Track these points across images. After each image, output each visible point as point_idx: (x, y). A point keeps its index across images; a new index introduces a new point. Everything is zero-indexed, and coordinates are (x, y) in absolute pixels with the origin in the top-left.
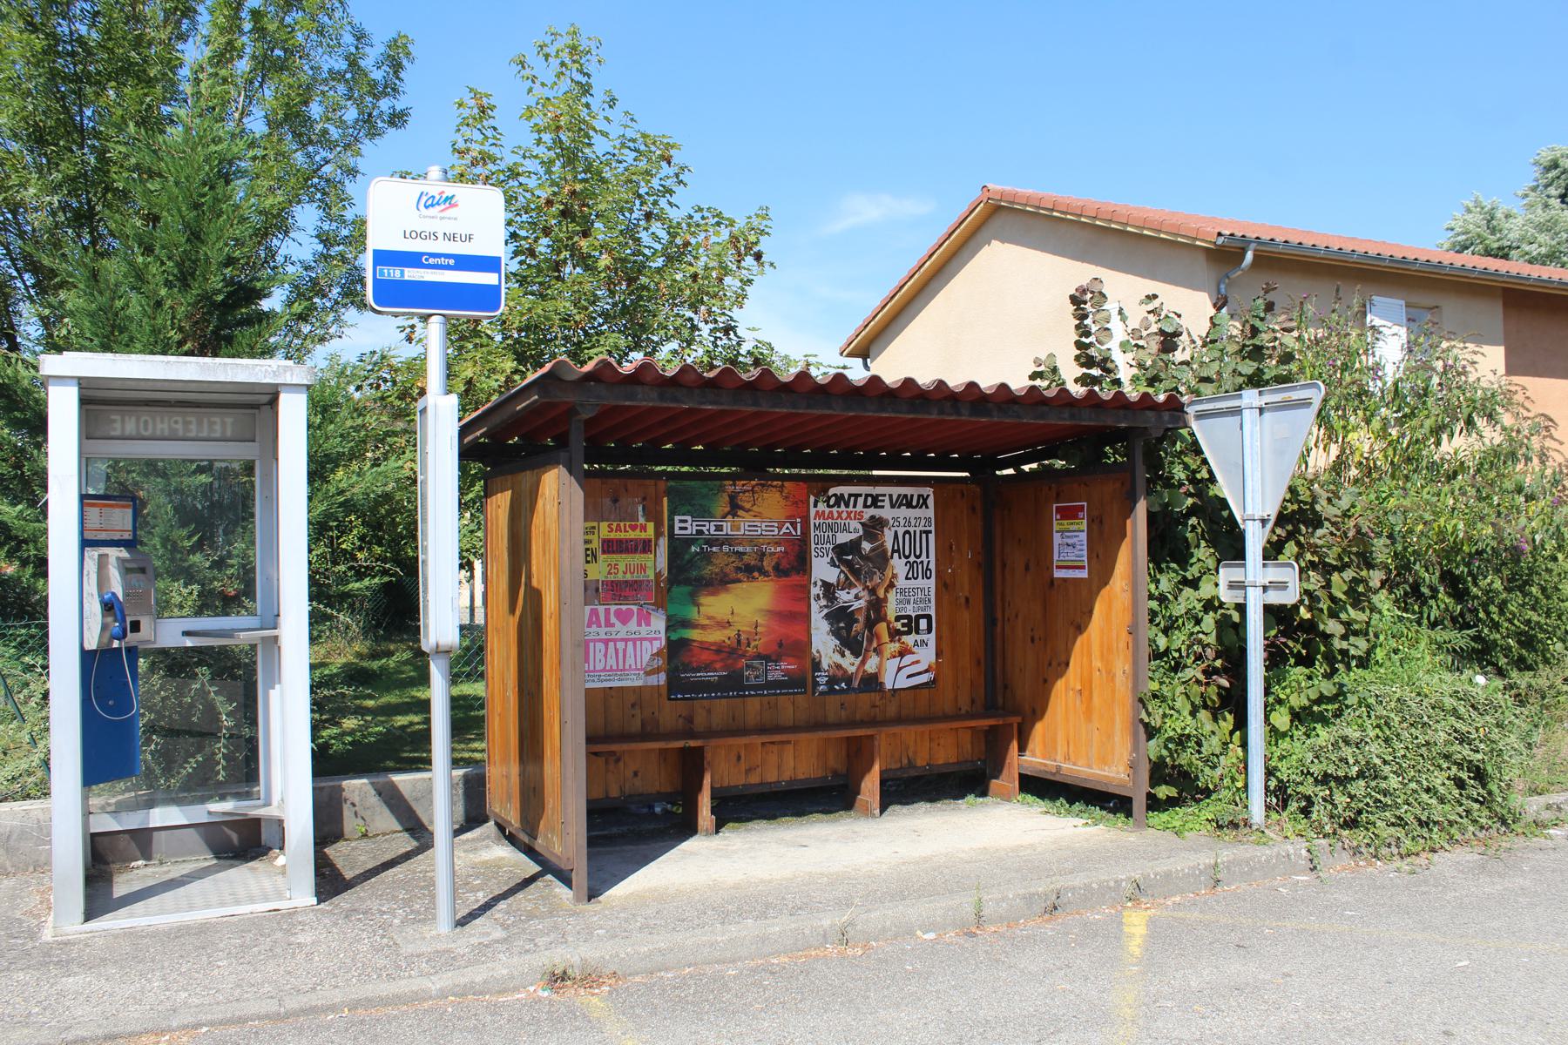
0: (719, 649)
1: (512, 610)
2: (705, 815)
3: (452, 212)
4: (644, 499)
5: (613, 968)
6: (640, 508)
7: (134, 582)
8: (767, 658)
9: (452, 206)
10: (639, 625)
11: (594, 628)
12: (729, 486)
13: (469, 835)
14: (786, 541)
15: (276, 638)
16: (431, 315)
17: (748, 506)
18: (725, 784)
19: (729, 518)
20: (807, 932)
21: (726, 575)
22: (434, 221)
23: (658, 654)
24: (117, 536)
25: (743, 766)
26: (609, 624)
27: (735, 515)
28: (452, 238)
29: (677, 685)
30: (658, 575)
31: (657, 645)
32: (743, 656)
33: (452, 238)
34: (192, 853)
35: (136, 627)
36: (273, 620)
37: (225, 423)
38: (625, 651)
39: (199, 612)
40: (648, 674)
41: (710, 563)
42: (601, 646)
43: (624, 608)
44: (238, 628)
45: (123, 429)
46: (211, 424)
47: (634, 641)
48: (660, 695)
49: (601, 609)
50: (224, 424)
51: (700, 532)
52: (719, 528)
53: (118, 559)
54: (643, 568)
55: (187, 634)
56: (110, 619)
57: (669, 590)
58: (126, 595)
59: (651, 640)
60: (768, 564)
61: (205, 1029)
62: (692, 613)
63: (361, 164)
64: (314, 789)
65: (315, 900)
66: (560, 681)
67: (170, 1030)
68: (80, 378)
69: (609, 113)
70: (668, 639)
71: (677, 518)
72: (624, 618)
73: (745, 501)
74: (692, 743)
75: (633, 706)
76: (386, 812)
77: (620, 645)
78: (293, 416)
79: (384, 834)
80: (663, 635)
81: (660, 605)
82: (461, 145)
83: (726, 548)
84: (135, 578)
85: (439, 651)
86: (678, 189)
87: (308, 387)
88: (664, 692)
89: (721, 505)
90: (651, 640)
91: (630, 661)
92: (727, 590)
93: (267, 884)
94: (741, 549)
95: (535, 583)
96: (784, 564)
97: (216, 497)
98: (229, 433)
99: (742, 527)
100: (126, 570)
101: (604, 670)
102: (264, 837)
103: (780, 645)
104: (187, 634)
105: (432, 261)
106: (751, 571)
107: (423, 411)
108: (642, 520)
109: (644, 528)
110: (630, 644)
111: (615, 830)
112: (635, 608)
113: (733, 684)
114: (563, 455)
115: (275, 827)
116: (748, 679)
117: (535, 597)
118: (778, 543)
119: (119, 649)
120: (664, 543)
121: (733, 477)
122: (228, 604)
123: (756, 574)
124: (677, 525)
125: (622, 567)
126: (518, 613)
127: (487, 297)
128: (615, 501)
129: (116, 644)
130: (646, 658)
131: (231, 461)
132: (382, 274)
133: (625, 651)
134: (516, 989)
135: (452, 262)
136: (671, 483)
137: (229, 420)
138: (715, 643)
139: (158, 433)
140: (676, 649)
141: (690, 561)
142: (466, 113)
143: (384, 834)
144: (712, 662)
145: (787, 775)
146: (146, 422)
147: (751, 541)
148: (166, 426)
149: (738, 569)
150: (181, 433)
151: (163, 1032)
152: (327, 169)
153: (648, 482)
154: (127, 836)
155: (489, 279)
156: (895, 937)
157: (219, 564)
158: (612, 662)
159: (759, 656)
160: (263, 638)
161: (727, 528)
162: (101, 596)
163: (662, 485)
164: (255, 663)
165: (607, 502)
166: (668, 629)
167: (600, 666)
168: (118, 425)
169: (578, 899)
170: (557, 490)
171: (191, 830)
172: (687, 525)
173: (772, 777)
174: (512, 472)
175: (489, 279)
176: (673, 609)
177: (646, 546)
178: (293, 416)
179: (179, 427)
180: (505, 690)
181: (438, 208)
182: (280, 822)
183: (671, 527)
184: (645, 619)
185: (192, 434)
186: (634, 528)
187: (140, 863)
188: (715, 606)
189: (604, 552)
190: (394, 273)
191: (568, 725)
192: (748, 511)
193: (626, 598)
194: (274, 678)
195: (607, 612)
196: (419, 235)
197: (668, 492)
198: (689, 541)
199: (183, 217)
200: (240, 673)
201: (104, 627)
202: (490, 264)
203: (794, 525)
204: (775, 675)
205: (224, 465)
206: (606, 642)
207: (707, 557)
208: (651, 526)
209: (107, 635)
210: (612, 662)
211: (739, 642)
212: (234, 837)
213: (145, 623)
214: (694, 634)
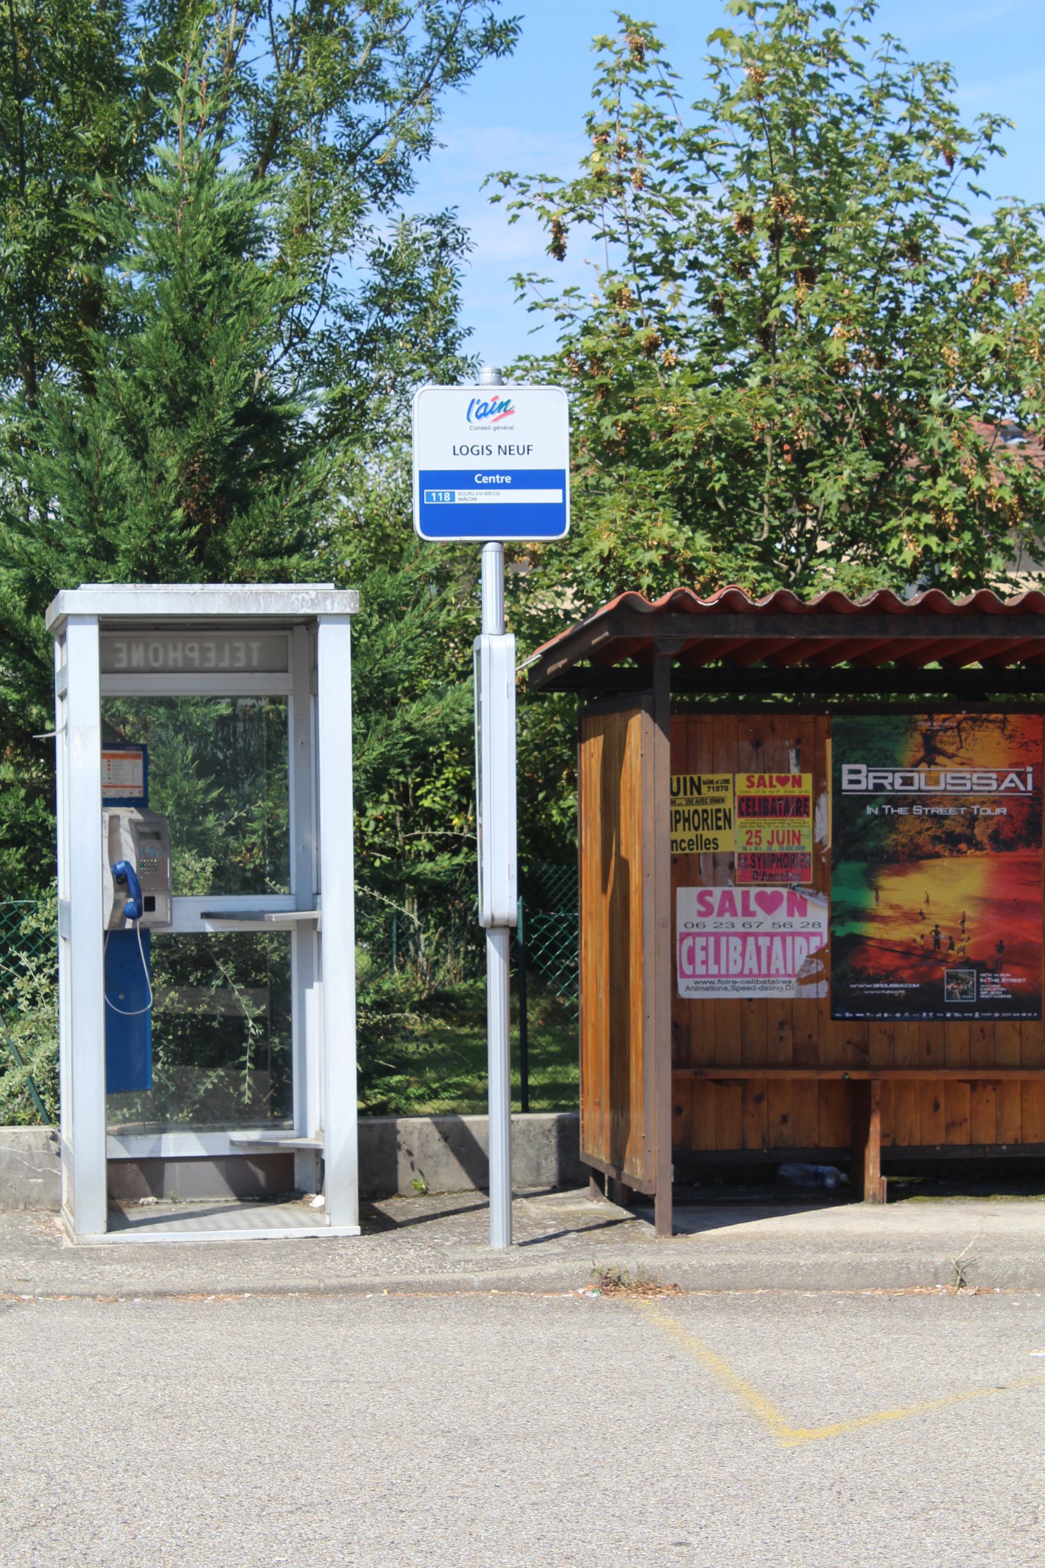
0: (907, 950)
1: (604, 890)
2: (873, 1177)
3: (506, 421)
4: (798, 741)
5: (675, 1280)
6: (792, 754)
7: (148, 850)
8: (980, 966)
9: (508, 412)
10: (791, 914)
12: (923, 722)
13: (560, 1195)
14: (1010, 799)
15: (315, 922)
16: (487, 542)
17: (951, 749)
18: (916, 1142)
19: (923, 767)
20: (913, 1267)
21: (918, 847)
22: (489, 433)
23: (819, 954)
24: (126, 794)
25: (943, 1118)
26: (747, 912)
27: (931, 762)
28: (507, 451)
29: (842, 999)
30: (818, 846)
31: (815, 943)
32: (944, 961)
33: (507, 451)
34: (211, 1193)
35: (150, 904)
36: (313, 898)
37: (250, 649)
39: (215, 890)
40: (802, 982)
41: (893, 829)
42: (736, 942)
43: (769, 890)
44: (273, 909)
45: (129, 660)
46: (234, 650)
47: (783, 936)
48: (821, 1013)
49: (737, 892)
50: (249, 650)
51: (879, 787)
52: (907, 781)
53: (131, 821)
54: (797, 837)
55: (207, 916)
56: (122, 895)
57: (834, 868)
58: (140, 865)
59: (807, 936)
60: (980, 832)
61: (247, 1295)
62: (868, 900)
64: (360, 1127)
65: (357, 1230)
66: (643, 967)
67: (214, 1292)
68: (99, 615)
69: (862, 29)
70: (832, 935)
71: (845, 768)
72: (769, 904)
73: (947, 742)
74: (854, 1075)
75: (781, 1025)
76: (455, 1164)
77: (764, 942)
78: (334, 650)
79: (450, 1193)
80: (824, 929)
81: (820, 887)
82: (603, 119)
83: (917, 810)
84: (149, 844)
85: (494, 926)
86: (992, 160)
87: (352, 615)
88: (827, 1008)
89: (912, 747)
90: (807, 936)
91: (777, 964)
92: (920, 869)
93: (303, 1217)
94: (940, 811)
95: (623, 853)
96: (1007, 833)
97: (241, 744)
98: (255, 662)
99: (947, 778)
100: (140, 835)
101: (741, 975)
102: (297, 1178)
103: (1000, 947)
104: (207, 916)
105: (485, 480)
106: (955, 841)
107: (479, 652)
108: (795, 771)
109: (797, 782)
110: (777, 940)
111: (757, 1197)
112: (784, 891)
113: (928, 1000)
115: (312, 1166)
116: (950, 994)
118: (996, 802)
119: (133, 931)
120: (826, 802)
121: (930, 709)
122: (254, 883)
123: (963, 846)
124: (846, 777)
125: (766, 835)
126: (609, 891)
128: (757, 744)
129: (129, 924)
130: (801, 960)
131: (258, 698)
132: (430, 498)
133: (770, 949)
134: (564, 1290)
135: (508, 479)
136: (838, 720)
137: (255, 645)
138: (900, 943)
139: (171, 663)
140: (843, 952)
141: (864, 827)
142: (610, 59)
143: (450, 1193)
144: (898, 969)
145: (1010, 1136)
146: (156, 650)
147: (956, 800)
148: (179, 654)
149: (935, 839)
150: (197, 664)
151: (209, 1293)
152: (379, 144)
153: (804, 718)
154: (135, 1167)
155: (551, 496)
156: (1031, 1287)
157: (236, 830)
158: (751, 964)
159: (967, 963)
160: (299, 922)
161: (920, 780)
162: (113, 867)
163: (824, 722)
164: (288, 966)
165: (746, 746)
166: (832, 921)
167: (735, 970)
168: (123, 655)
169: (660, 1232)
170: (643, 737)
171: (210, 1164)
172: (861, 777)
173: (986, 1136)
175: (551, 496)
176: (839, 893)
177: (800, 807)
178: (334, 650)
179: (196, 655)
180: (598, 992)
181: (491, 417)
182: (318, 1153)
183: (837, 781)
184: (798, 906)
185: (211, 664)
186: (783, 782)
187: (151, 1199)
188: (901, 890)
189: (741, 814)
190: (443, 496)
191: (651, 1022)
192: (951, 756)
193: (772, 877)
194: (314, 971)
195: (746, 896)
197: (832, 732)
198: (863, 800)
199: (174, 321)
200: (269, 971)
201: (116, 904)
202: (550, 479)
203: (1022, 777)
204: (993, 989)
205: (249, 702)
206: (744, 937)
207: (890, 822)
208: (807, 779)
209: (119, 913)
210: (751, 964)
211: (937, 942)
212: (261, 1175)
213: (159, 903)
214: (870, 930)
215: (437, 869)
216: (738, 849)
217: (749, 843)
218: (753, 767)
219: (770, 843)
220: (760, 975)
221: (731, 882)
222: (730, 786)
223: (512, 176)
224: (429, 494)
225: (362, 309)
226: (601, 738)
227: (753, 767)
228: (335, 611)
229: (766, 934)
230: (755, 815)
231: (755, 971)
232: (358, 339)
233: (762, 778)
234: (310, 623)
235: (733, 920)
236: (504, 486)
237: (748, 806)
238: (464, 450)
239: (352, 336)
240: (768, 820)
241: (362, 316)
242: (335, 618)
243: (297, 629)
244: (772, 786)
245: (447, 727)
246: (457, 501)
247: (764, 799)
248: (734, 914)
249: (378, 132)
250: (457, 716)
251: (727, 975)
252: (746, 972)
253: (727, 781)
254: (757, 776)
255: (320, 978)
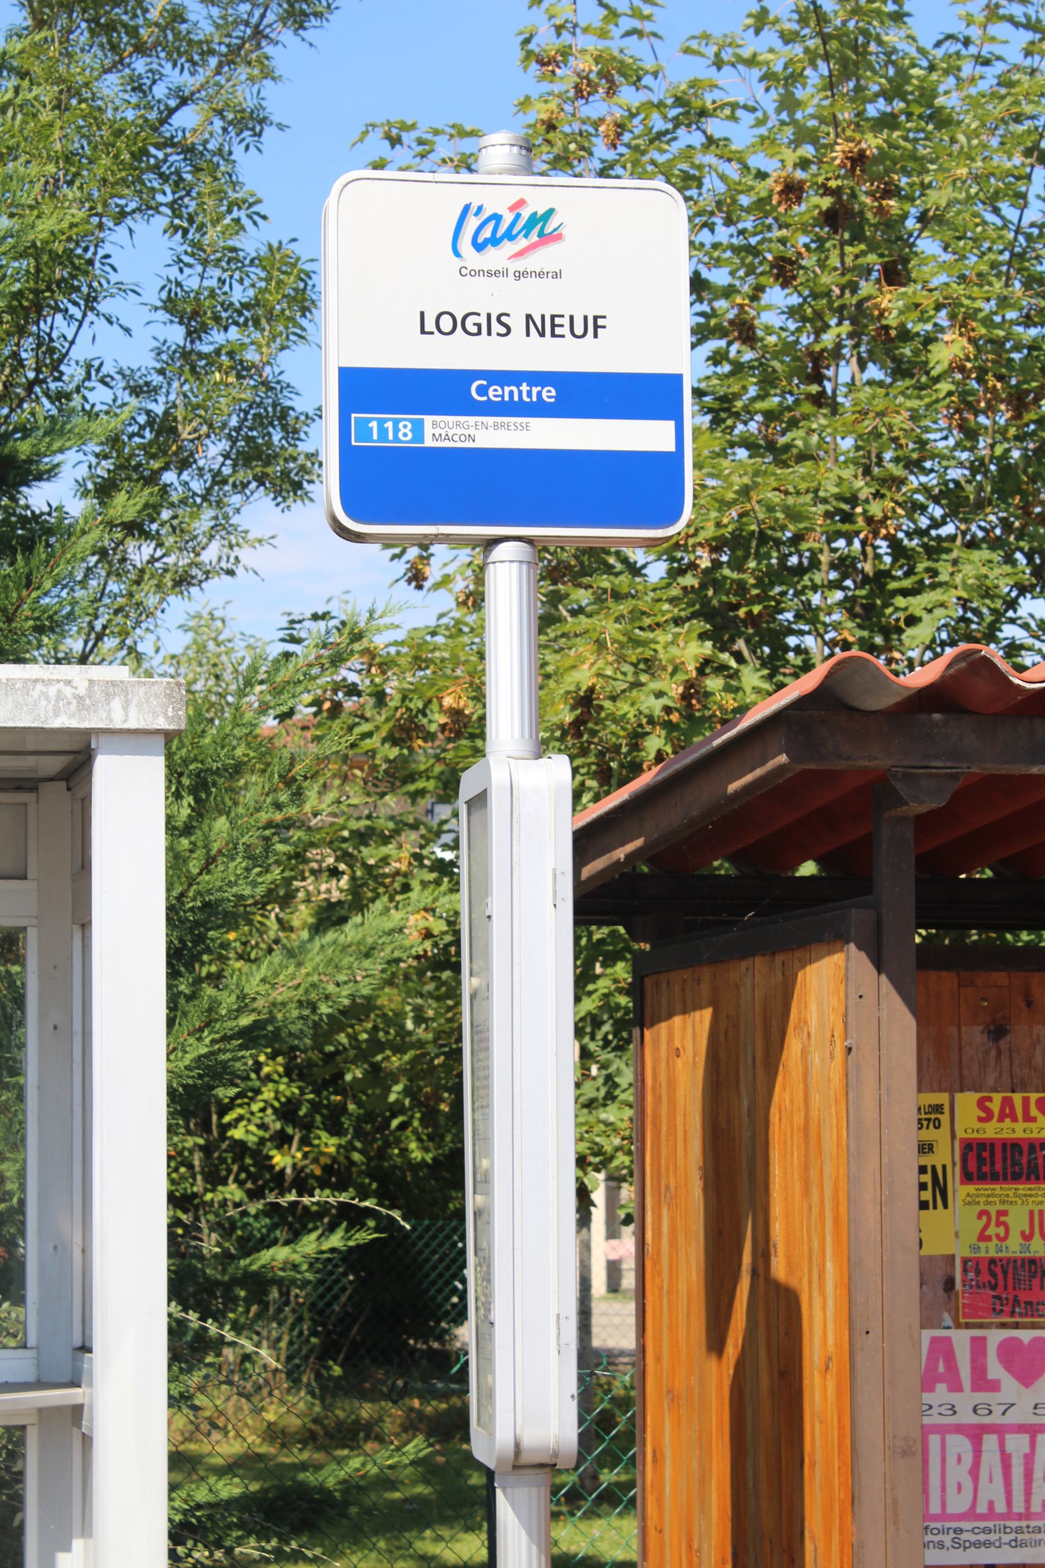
1: (716, 1343)
3: (544, 258)
11: (941, 1393)
15: (77, 1412)
16: (493, 542)
26: (982, 1382)
38: (1029, 1460)
42: (960, 1444)
43: (1026, 1336)
49: (961, 1339)
63: (274, 99)
77: (1016, 1444)
78: (129, 813)
82: (546, 41)
85: (520, 1463)
87: (168, 736)
95: (779, 1269)
101: (971, 1514)
107: (480, 801)
114: (857, 916)
117: (780, 1312)
125: (1018, 1220)
126: (732, 1349)
127: (644, 485)
128: (998, 1032)
132: (365, 432)
135: (549, 394)
152: (187, 119)
155: (652, 436)
158: (992, 1491)
160: (44, 1413)
165: (976, 1035)
167: (958, 1504)
170: (840, 1010)
174: (716, 960)
175: (652, 436)
178: (129, 813)
181: (510, 248)
189: (967, 1178)
190: (394, 430)
194: (75, 1517)
195: (978, 1346)
196: (459, 324)
206: (976, 1434)
215: (297, 1258)
216: (961, 1251)
217: (983, 1237)
218: (990, 1080)
219: (1027, 1237)
220: (1009, 1515)
221: (948, 1320)
222: (945, 1119)
223: (405, 127)
224: (363, 424)
225: (157, 379)
226: (706, 1015)
227: (990, 1080)
228: (133, 723)
229: (1021, 1428)
230: (994, 1178)
231: (1000, 1507)
232: (150, 423)
233: (1007, 1102)
234: (72, 763)
235: (954, 1398)
236: (539, 410)
237: (980, 1159)
238: (446, 323)
239: (142, 419)
240: (1022, 1188)
241: (156, 390)
242: (133, 739)
243: (46, 788)
244: (1028, 1118)
245: (314, 1009)
246: (429, 442)
247: (1013, 1146)
248: (956, 1387)
249: (184, 102)
250: (331, 988)
251: (943, 1516)
252: (982, 1508)
253: (938, 1109)
254: (997, 1098)
255: (86, 1531)
